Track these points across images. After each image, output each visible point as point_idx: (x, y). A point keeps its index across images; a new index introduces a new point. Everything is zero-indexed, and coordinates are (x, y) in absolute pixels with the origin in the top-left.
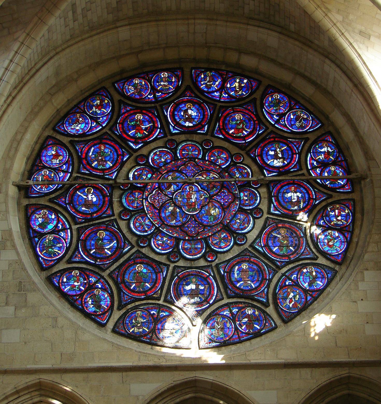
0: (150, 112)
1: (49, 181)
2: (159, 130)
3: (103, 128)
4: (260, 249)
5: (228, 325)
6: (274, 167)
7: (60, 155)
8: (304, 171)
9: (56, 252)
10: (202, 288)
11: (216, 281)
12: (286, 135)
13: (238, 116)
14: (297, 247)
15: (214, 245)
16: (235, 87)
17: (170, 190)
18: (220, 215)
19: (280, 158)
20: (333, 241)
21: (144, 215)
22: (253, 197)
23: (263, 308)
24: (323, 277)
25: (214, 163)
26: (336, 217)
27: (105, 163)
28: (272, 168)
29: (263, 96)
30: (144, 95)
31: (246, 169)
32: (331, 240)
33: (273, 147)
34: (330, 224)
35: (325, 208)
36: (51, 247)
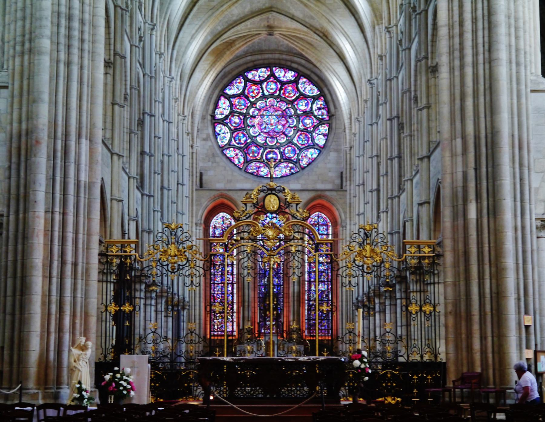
1: (222, 114)
10: (274, 156)
14: (308, 141)
21: (255, 128)
22: (293, 122)
25: (280, 107)
28: (300, 110)
29: (299, 79)
35: (318, 126)
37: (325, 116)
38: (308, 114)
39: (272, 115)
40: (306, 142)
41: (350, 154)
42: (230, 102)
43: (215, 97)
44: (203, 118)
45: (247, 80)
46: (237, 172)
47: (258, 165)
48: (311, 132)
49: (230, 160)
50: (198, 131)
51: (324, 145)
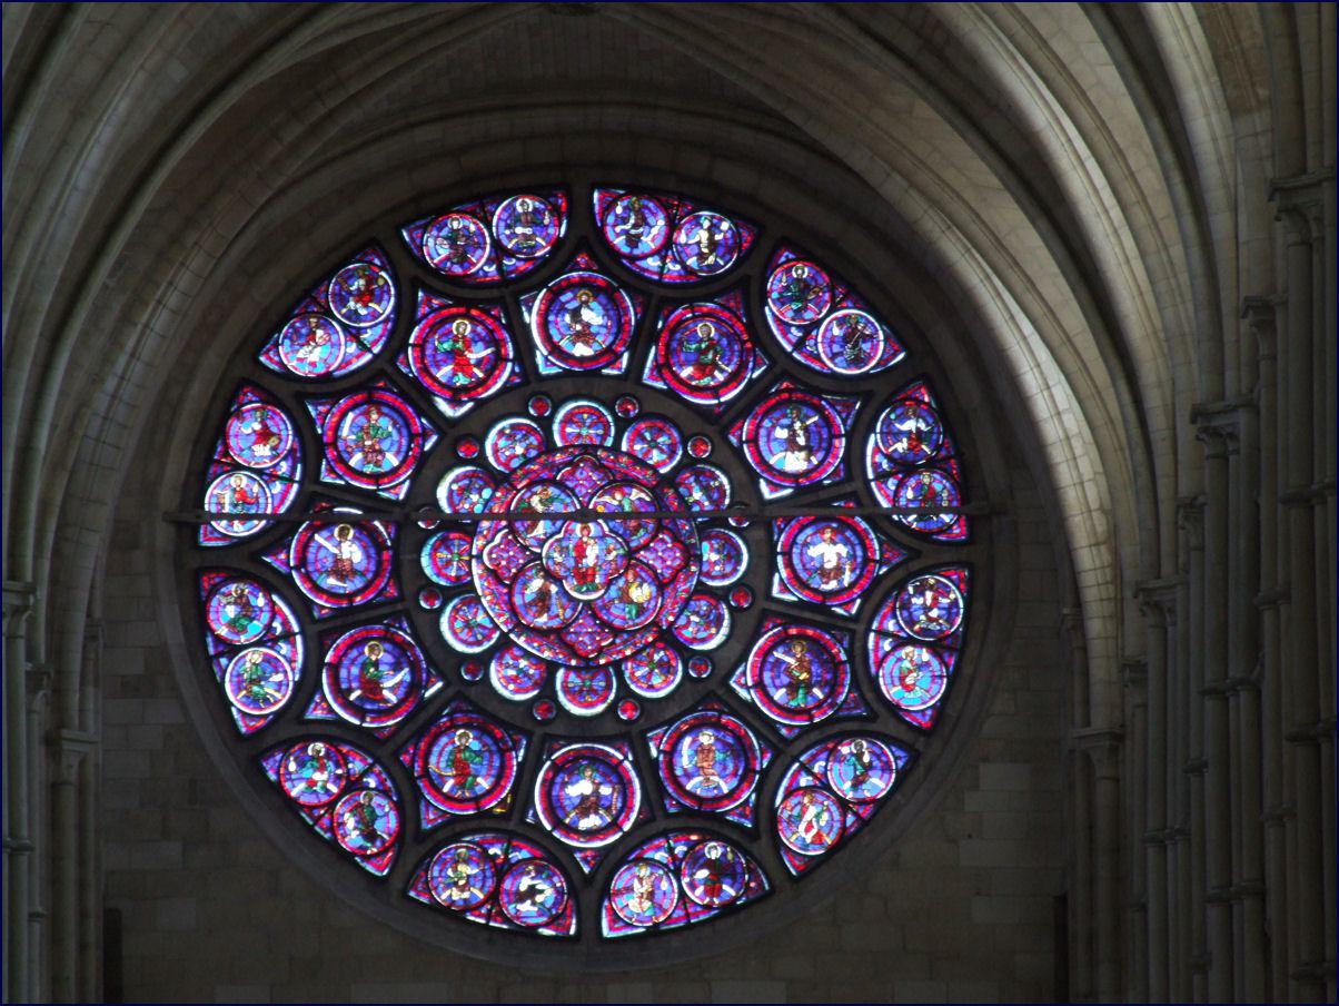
0: (487, 313)
2: (510, 365)
3: (376, 357)
4: (743, 693)
5: (664, 885)
6: (783, 475)
7: (273, 434)
8: (857, 485)
9: (267, 693)
10: (606, 790)
11: (639, 775)
12: (818, 382)
13: (704, 329)
14: (832, 692)
15: (636, 681)
16: (699, 243)
17: (534, 534)
18: (653, 603)
19: (801, 449)
20: (915, 674)
23: (746, 844)
24: (886, 768)
26: (926, 609)
27: (379, 458)
28: (779, 477)
29: (769, 267)
30: (475, 265)
31: (715, 478)
32: (910, 671)
33: (785, 416)
34: (911, 628)
35: (902, 586)
36: (256, 681)
37: (946, 518)
39: (585, 516)
40: (817, 692)
41: (1117, 780)
42: (303, 427)
43: (198, 392)
44: (124, 539)
45: (415, 276)
47: (492, 851)
48: (853, 631)
50: (90, 637)
51: (940, 709)
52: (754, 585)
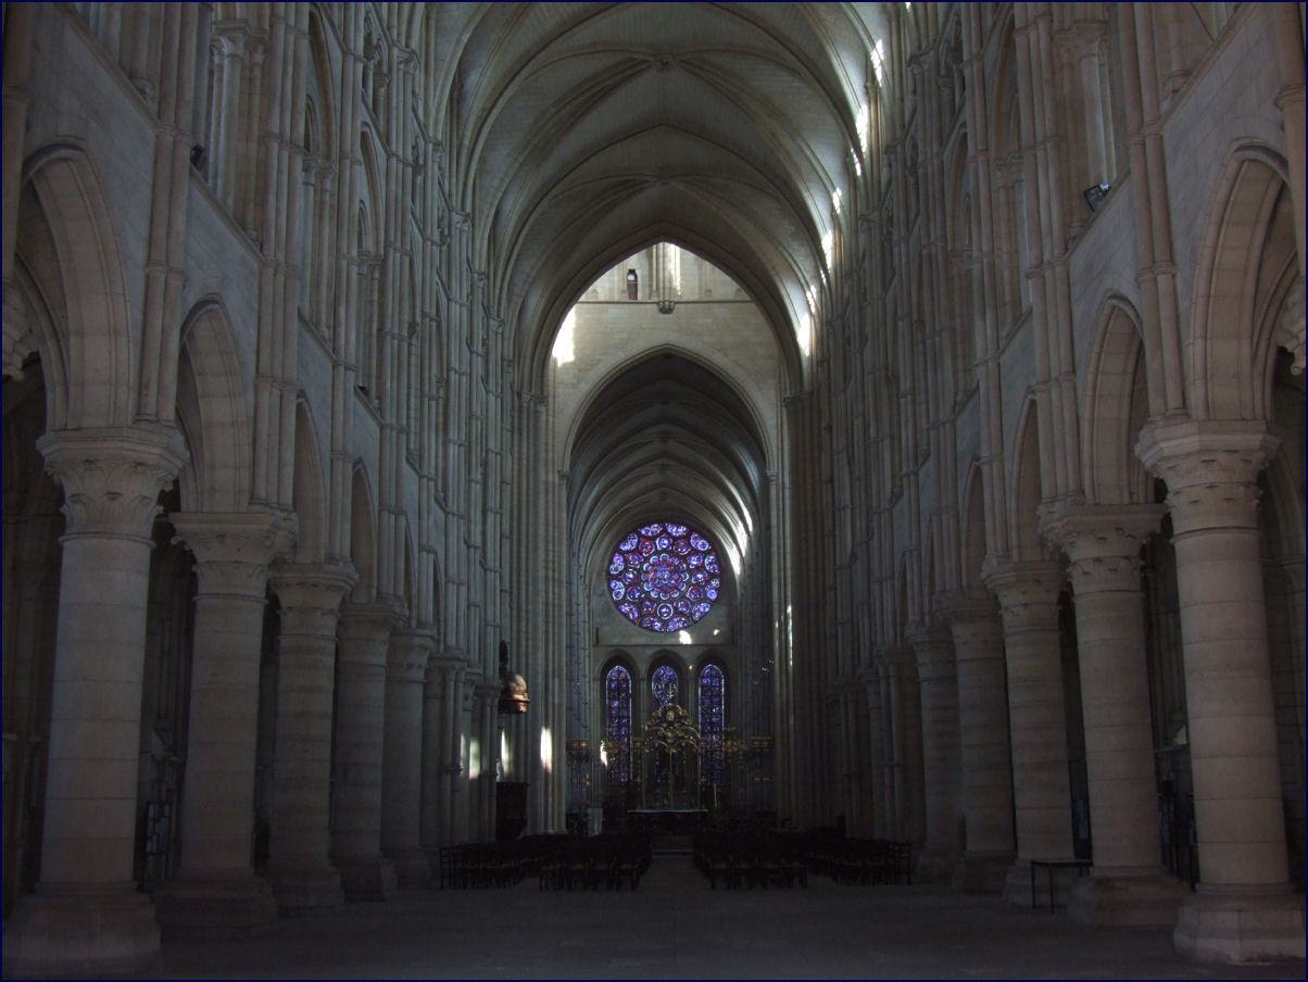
1: (616, 569)
38: (700, 568)
44: (599, 574)
45: (640, 535)
46: (632, 626)
49: (626, 615)
52: (689, 581)
